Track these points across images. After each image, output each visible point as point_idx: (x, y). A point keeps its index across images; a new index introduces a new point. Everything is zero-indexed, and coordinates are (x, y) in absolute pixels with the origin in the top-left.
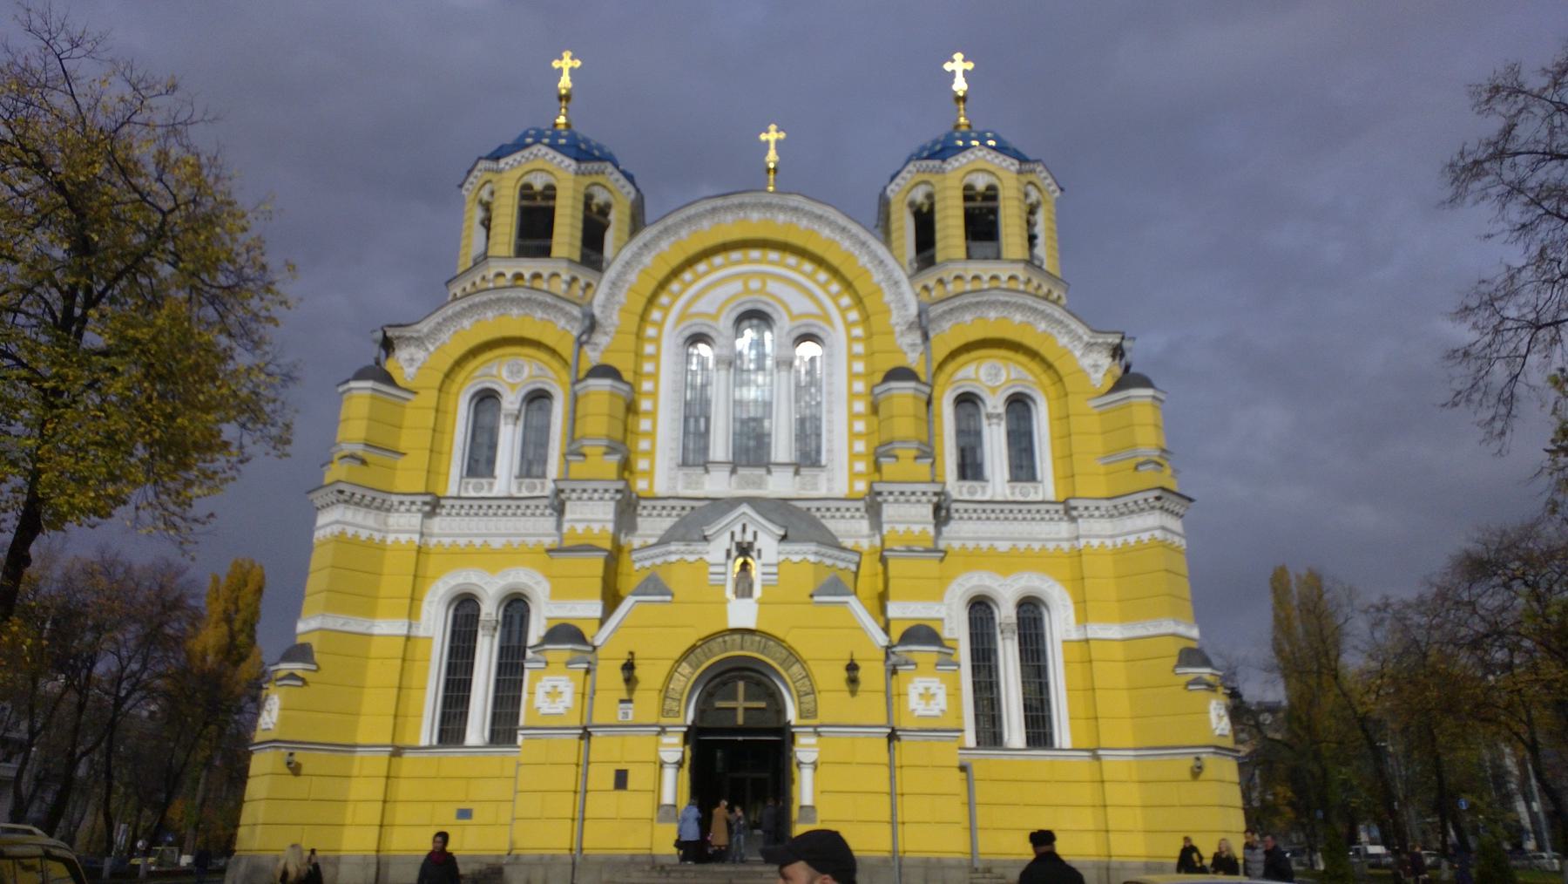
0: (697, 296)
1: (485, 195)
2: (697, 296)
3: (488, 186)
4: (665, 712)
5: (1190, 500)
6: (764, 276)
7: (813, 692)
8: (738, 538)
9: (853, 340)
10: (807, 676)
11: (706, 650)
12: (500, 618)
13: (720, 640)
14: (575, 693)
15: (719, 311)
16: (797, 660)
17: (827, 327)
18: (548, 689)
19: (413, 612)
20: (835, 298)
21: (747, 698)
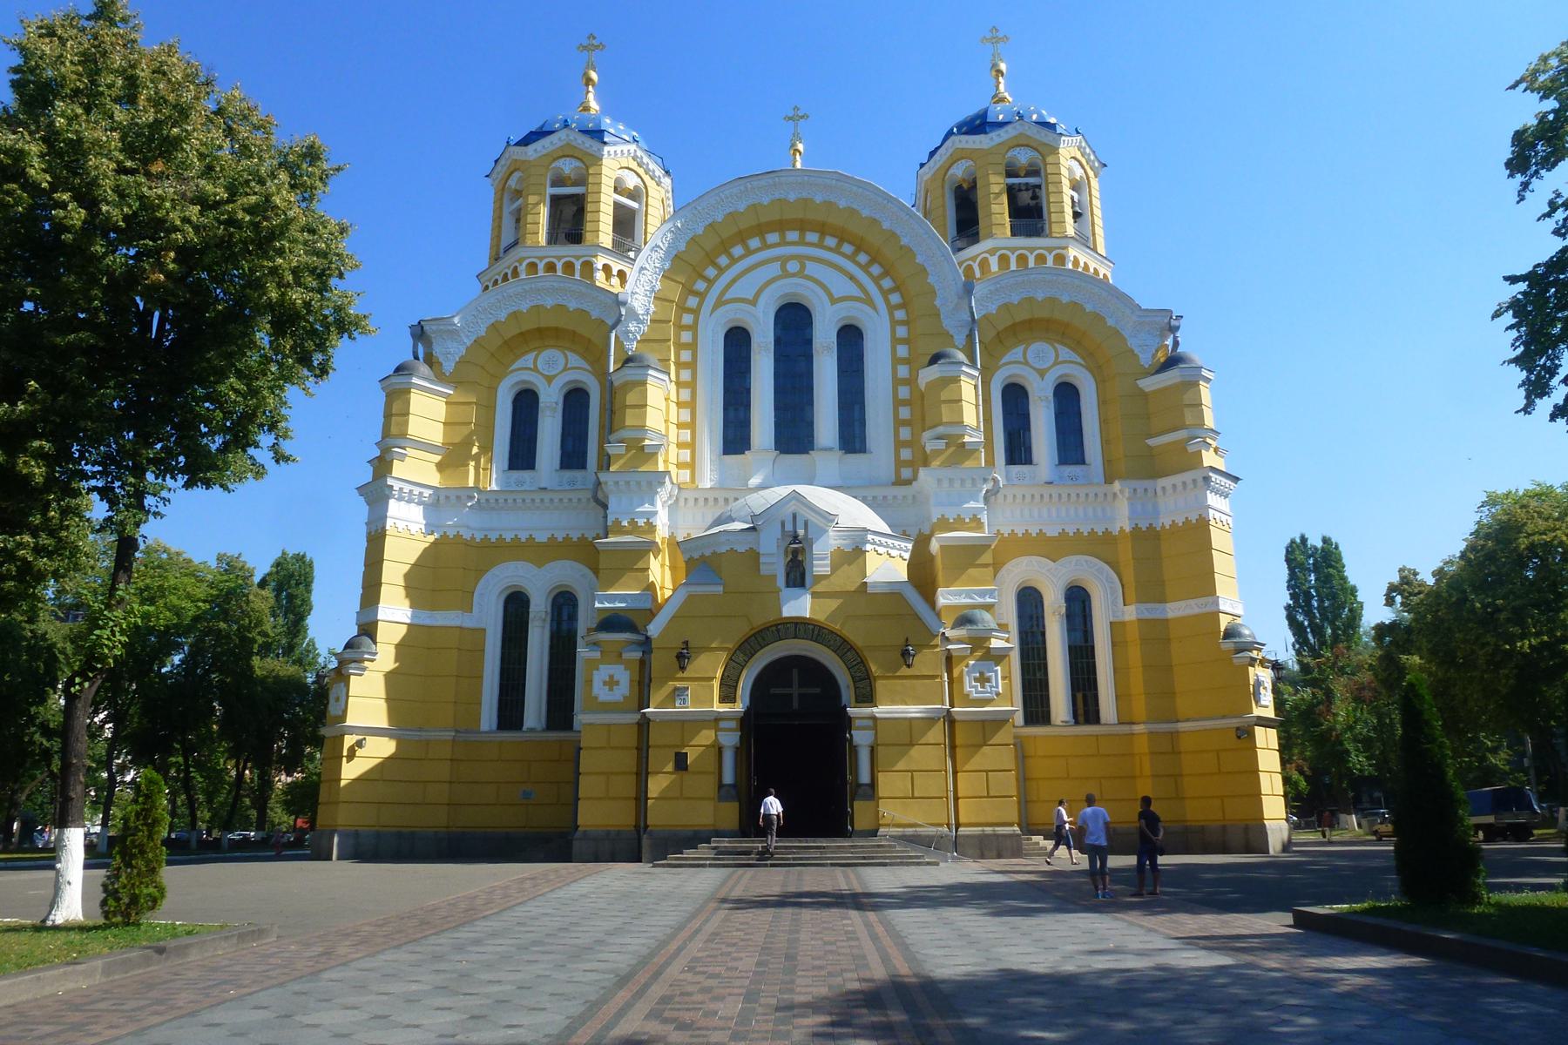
0: (734, 281)
1: (513, 183)
2: (734, 281)
3: (517, 175)
4: (723, 700)
5: (1236, 479)
6: (801, 259)
7: (869, 678)
8: (789, 527)
9: (894, 323)
10: (862, 662)
11: (760, 639)
12: (549, 610)
13: (774, 628)
14: (631, 681)
15: (758, 295)
16: (852, 647)
17: (868, 309)
18: (607, 679)
19: (468, 608)
20: (876, 280)
21: (800, 686)
